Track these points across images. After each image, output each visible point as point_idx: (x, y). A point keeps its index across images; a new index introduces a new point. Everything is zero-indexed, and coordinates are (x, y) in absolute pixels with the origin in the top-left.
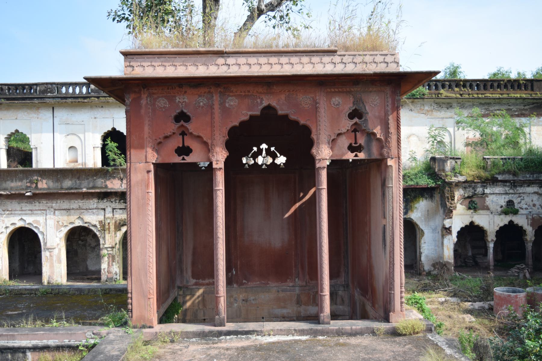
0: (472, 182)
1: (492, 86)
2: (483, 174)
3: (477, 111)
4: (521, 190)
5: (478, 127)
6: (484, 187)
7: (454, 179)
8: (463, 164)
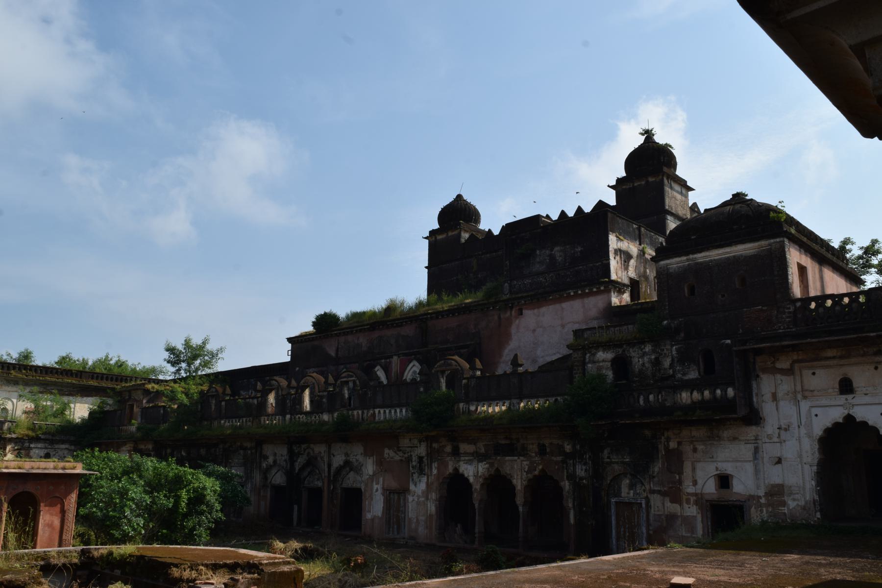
0: (22, 438)
1: (51, 372)
2: (31, 433)
3: (36, 389)
4: (56, 446)
5: (34, 401)
6: (30, 443)
7: (9, 436)
8: (17, 426)
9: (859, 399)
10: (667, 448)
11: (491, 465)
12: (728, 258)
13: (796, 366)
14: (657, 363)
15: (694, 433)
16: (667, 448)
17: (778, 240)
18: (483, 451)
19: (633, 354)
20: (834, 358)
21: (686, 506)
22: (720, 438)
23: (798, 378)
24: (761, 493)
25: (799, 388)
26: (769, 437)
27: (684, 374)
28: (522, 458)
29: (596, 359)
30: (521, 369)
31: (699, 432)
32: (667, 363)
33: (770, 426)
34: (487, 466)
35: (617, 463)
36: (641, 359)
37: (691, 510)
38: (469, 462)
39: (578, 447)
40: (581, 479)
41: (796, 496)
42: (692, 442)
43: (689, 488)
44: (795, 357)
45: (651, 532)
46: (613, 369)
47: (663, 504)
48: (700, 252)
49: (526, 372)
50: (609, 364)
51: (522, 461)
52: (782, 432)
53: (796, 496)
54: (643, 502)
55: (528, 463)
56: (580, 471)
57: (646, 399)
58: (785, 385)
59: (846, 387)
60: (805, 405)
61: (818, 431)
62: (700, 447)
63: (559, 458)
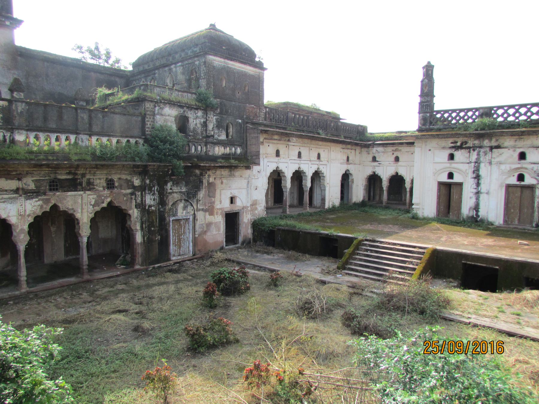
9: (281, 159)
10: (208, 182)
11: (47, 201)
12: (242, 71)
14: (205, 125)
15: (223, 173)
16: (208, 182)
18: (32, 186)
19: (190, 116)
21: (216, 216)
24: (249, 205)
27: (219, 136)
29: (163, 113)
31: (225, 172)
32: (210, 126)
34: (40, 203)
35: (176, 193)
36: (195, 120)
38: (12, 200)
39: (148, 182)
40: (150, 206)
42: (221, 178)
43: (218, 206)
45: (197, 236)
47: (205, 217)
48: (231, 60)
50: (173, 119)
51: (88, 195)
55: (95, 196)
56: (150, 200)
57: (196, 149)
61: (268, 174)
62: (225, 181)
63: (129, 191)
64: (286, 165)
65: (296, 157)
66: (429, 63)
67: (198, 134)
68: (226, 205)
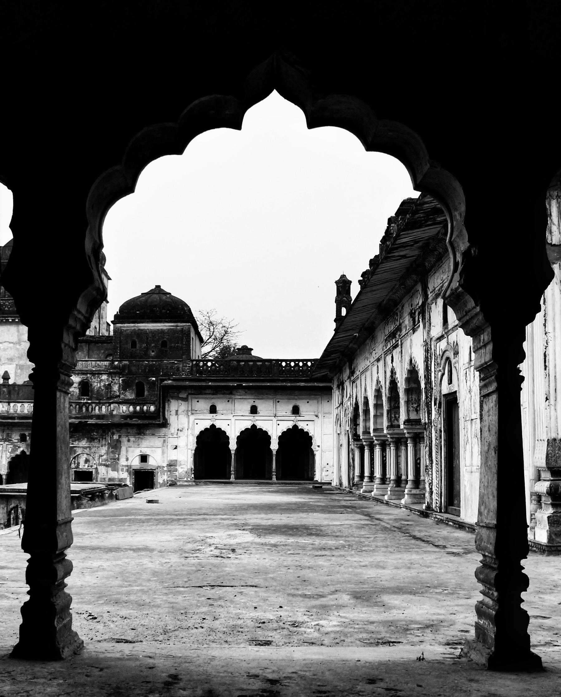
9: (219, 416)
12: (158, 330)
13: (190, 397)
17: (188, 324)
20: (209, 394)
21: (120, 472)
22: (145, 434)
23: (190, 403)
25: (190, 409)
26: (172, 434)
28: (7, 443)
30: (11, 382)
33: (173, 429)
37: (124, 475)
41: (183, 466)
43: (123, 462)
44: (190, 392)
46: (79, 389)
47: (107, 472)
49: (14, 385)
52: (179, 432)
53: (183, 466)
54: (94, 471)
58: (182, 406)
59: (213, 410)
60: (192, 418)
61: (197, 433)
62: (132, 439)
64: (229, 422)
65: (247, 413)
66: (343, 276)
67: (102, 395)
68: (136, 463)
